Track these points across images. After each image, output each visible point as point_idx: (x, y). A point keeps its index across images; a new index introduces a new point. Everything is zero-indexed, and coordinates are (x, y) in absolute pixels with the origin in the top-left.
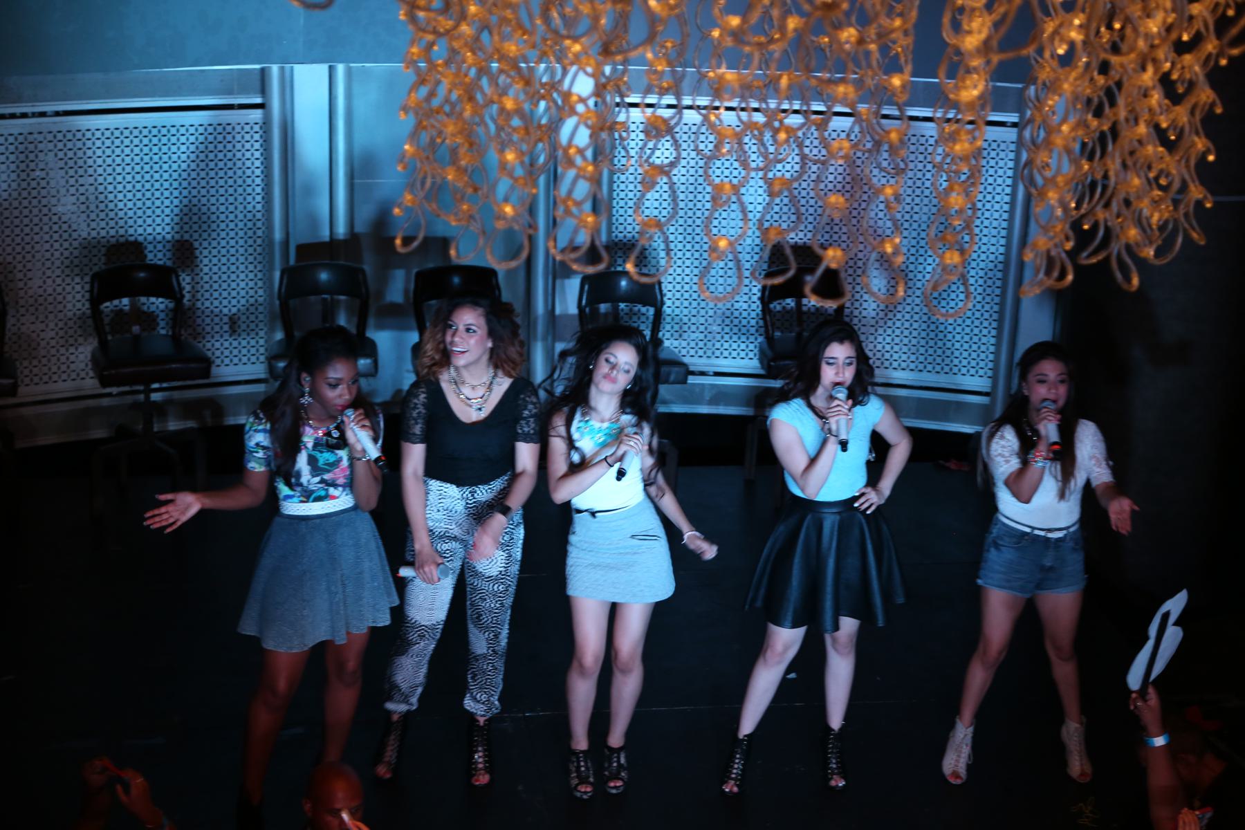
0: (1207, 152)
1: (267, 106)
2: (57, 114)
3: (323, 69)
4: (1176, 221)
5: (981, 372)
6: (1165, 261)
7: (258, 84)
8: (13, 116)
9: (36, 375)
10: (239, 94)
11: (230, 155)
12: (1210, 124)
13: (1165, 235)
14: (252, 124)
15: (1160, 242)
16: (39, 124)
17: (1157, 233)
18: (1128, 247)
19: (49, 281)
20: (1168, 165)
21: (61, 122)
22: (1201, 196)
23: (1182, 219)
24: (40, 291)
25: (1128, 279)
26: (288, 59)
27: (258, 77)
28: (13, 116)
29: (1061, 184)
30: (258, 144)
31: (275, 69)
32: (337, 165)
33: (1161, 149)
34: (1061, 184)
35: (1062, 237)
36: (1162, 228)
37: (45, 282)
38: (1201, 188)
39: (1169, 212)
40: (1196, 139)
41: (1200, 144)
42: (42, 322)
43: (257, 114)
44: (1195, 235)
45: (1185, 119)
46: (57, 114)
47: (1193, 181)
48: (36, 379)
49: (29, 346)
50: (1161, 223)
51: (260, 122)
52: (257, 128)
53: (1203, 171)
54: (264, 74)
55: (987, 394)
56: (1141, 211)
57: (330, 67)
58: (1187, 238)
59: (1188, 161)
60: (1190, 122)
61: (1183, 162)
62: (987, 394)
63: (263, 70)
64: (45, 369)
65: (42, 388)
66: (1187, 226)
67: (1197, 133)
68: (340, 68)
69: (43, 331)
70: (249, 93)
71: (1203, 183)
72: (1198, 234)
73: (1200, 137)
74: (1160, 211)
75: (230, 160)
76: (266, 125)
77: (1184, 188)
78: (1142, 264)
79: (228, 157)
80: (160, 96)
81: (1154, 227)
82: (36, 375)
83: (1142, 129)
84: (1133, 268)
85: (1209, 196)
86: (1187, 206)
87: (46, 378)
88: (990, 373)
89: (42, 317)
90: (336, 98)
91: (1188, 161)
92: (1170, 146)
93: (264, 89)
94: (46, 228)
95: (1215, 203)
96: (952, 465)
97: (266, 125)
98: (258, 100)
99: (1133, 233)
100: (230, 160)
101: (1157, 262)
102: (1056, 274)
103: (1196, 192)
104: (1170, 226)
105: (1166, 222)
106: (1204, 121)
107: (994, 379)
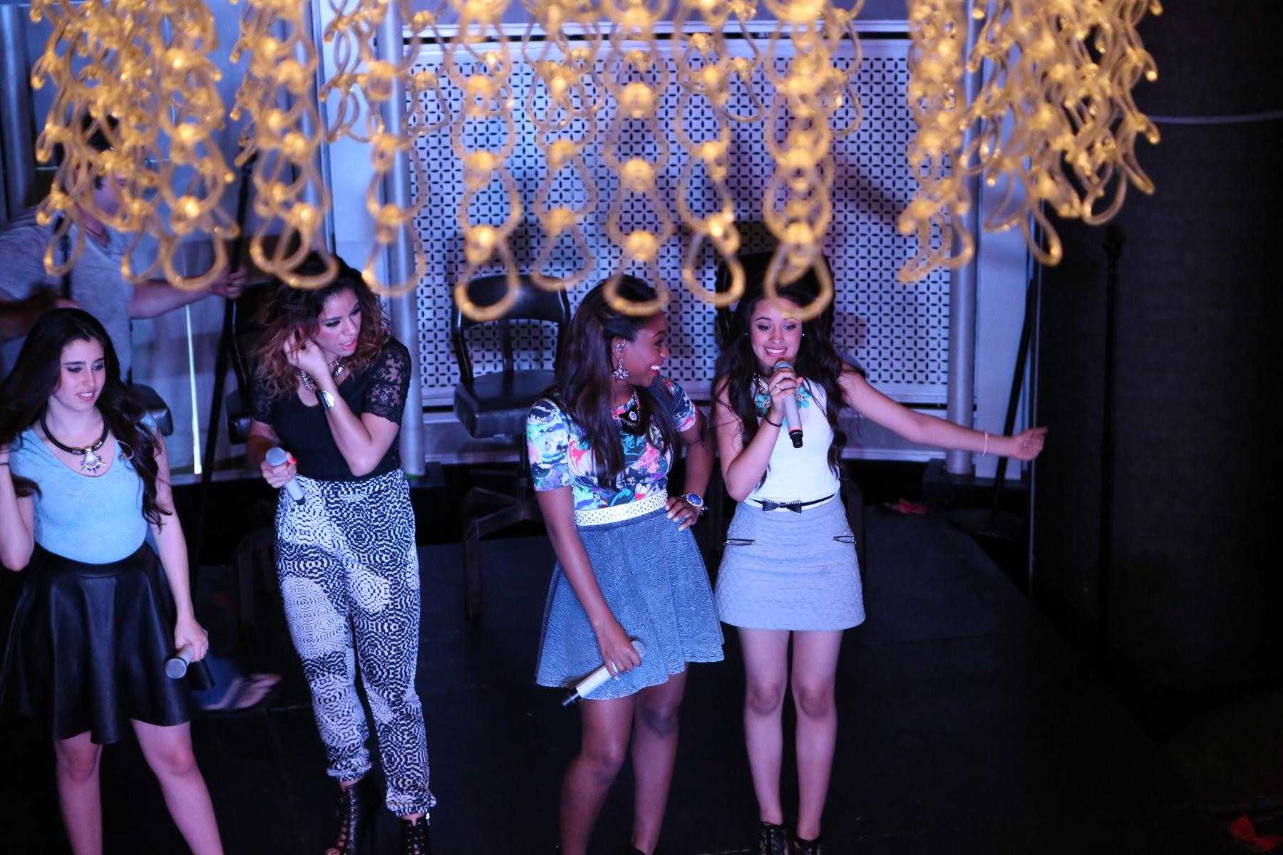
4: (1115, 163)
12: (1149, 31)
13: (1105, 181)
15: (1101, 193)
17: (1096, 180)
18: (1048, 209)
22: (1142, 128)
23: (1121, 161)
25: (1047, 249)
33: (1093, 66)
36: (1101, 171)
40: (1129, 50)
41: (1137, 56)
47: (1130, 109)
50: (1097, 167)
53: (1144, 95)
55: (943, 407)
56: (1064, 153)
59: (1120, 84)
60: (1113, 26)
62: (943, 407)
67: (1131, 44)
71: (1142, 108)
74: (1090, 149)
78: (1070, 229)
83: (1048, 43)
86: (1125, 140)
88: (944, 378)
91: (1120, 84)
92: (1096, 57)
96: (902, 507)
99: (1048, 187)
101: (1101, 220)
103: (1136, 123)
104: (1110, 172)
106: (1140, 28)
107: (950, 384)
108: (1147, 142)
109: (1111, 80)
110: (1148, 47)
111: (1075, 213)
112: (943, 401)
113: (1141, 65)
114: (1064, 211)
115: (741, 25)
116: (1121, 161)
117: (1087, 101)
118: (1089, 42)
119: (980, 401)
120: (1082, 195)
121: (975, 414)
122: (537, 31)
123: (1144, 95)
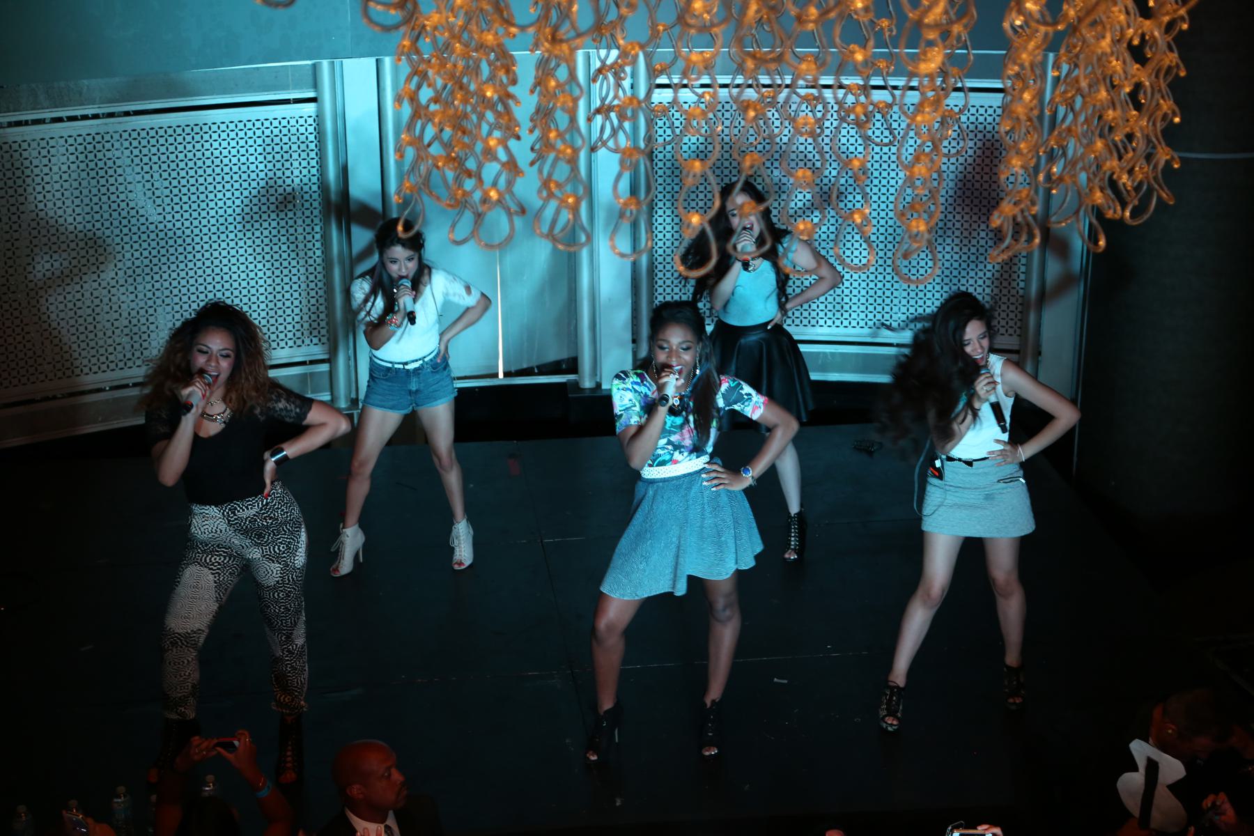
0: (1174, 114)
1: (319, 100)
2: (127, 114)
3: (370, 62)
5: (1011, 331)
6: (1141, 221)
7: (310, 79)
8: (85, 117)
9: (112, 362)
10: (293, 89)
11: (286, 148)
12: (1178, 89)
13: (1141, 194)
14: (306, 117)
15: (1136, 202)
16: (106, 124)
17: (1133, 194)
18: (1099, 213)
19: (121, 273)
20: (1132, 129)
21: (126, 122)
22: (1168, 157)
23: (1153, 182)
24: (113, 283)
25: (1096, 242)
26: (334, 55)
27: (310, 73)
28: (85, 117)
29: (1025, 151)
30: (313, 136)
31: (325, 64)
32: (387, 153)
33: (1134, 113)
34: (1025, 151)
35: (1029, 203)
36: (1137, 189)
37: (117, 274)
38: (1167, 149)
39: (1143, 173)
40: (1162, 101)
41: (1167, 105)
42: (116, 311)
43: (310, 108)
44: (1164, 195)
45: (1147, 84)
46: (127, 114)
47: (1160, 143)
48: (112, 366)
49: (105, 334)
50: (1136, 184)
51: (314, 116)
52: (310, 121)
53: (1171, 135)
54: (315, 69)
55: (1017, 352)
56: (1113, 174)
57: (377, 60)
58: (1159, 198)
59: (1154, 124)
61: (1151, 124)
62: (1017, 352)
63: (314, 66)
64: (120, 356)
65: (118, 374)
66: (1156, 186)
67: (1163, 97)
68: (388, 61)
69: (117, 320)
70: (301, 88)
71: (1170, 144)
72: (1167, 195)
73: (1165, 101)
74: (1131, 172)
75: (286, 152)
76: (319, 119)
77: (1154, 147)
79: (284, 150)
80: (217, 94)
81: (1129, 188)
82: (112, 362)
83: (1103, 94)
84: (1100, 229)
85: (1176, 156)
86: (1155, 166)
87: (121, 365)
88: (1018, 331)
89: (115, 307)
90: (384, 89)
91: (1154, 124)
92: (1138, 106)
93: (316, 85)
94: (116, 223)
95: (1182, 160)
97: (319, 119)
98: (311, 95)
99: (1098, 197)
100: (286, 152)
102: (1024, 238)
103: (1164, 155)
104: (1145, 187)
105: (1141, 183)
106: (1169, 86)
108: (1172, 166)
109: (1148, 122)
110: (1176, 102)
111: (1117, 216)
112: (1016, 348)
113: (1169, 112)
114: (1110, 214)
115: (884, 80)
116: (1153, 182)
117: (1130, 137)
118: (1133, 95)
119: (1045, 348)
120: (1124, 206)
121: (1040, 358)
122: (740, 80)
123: (1171, 135)
